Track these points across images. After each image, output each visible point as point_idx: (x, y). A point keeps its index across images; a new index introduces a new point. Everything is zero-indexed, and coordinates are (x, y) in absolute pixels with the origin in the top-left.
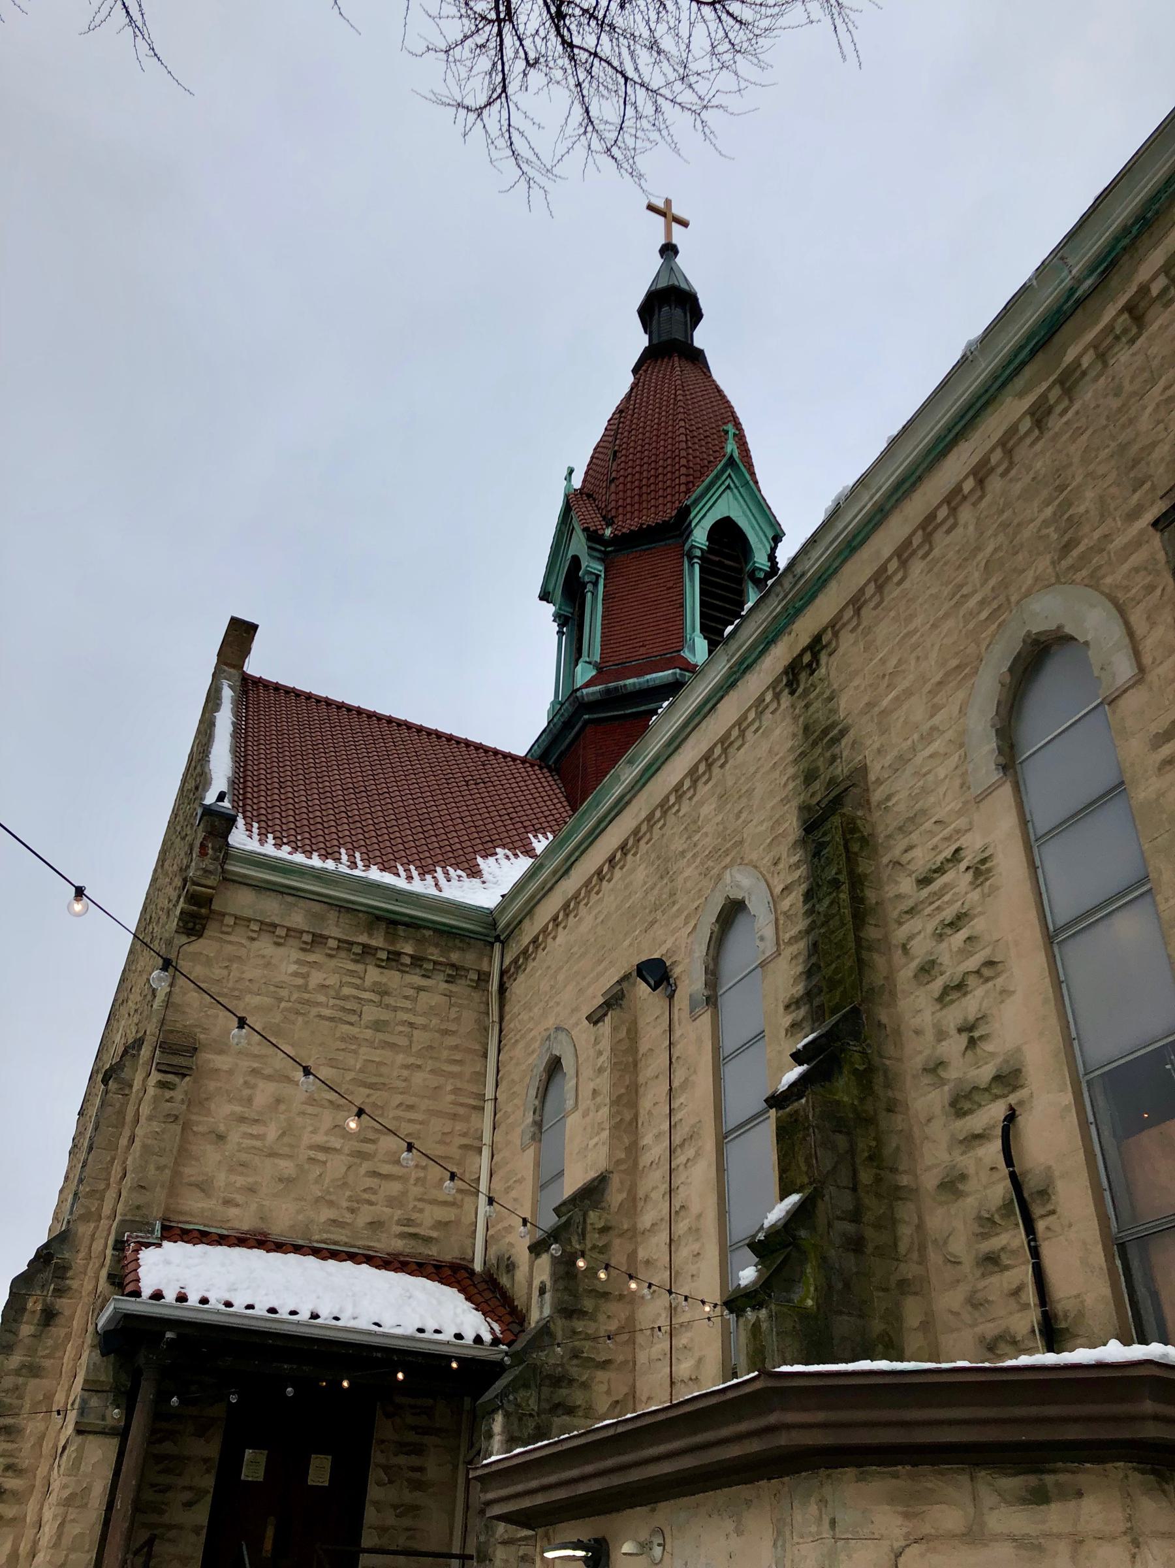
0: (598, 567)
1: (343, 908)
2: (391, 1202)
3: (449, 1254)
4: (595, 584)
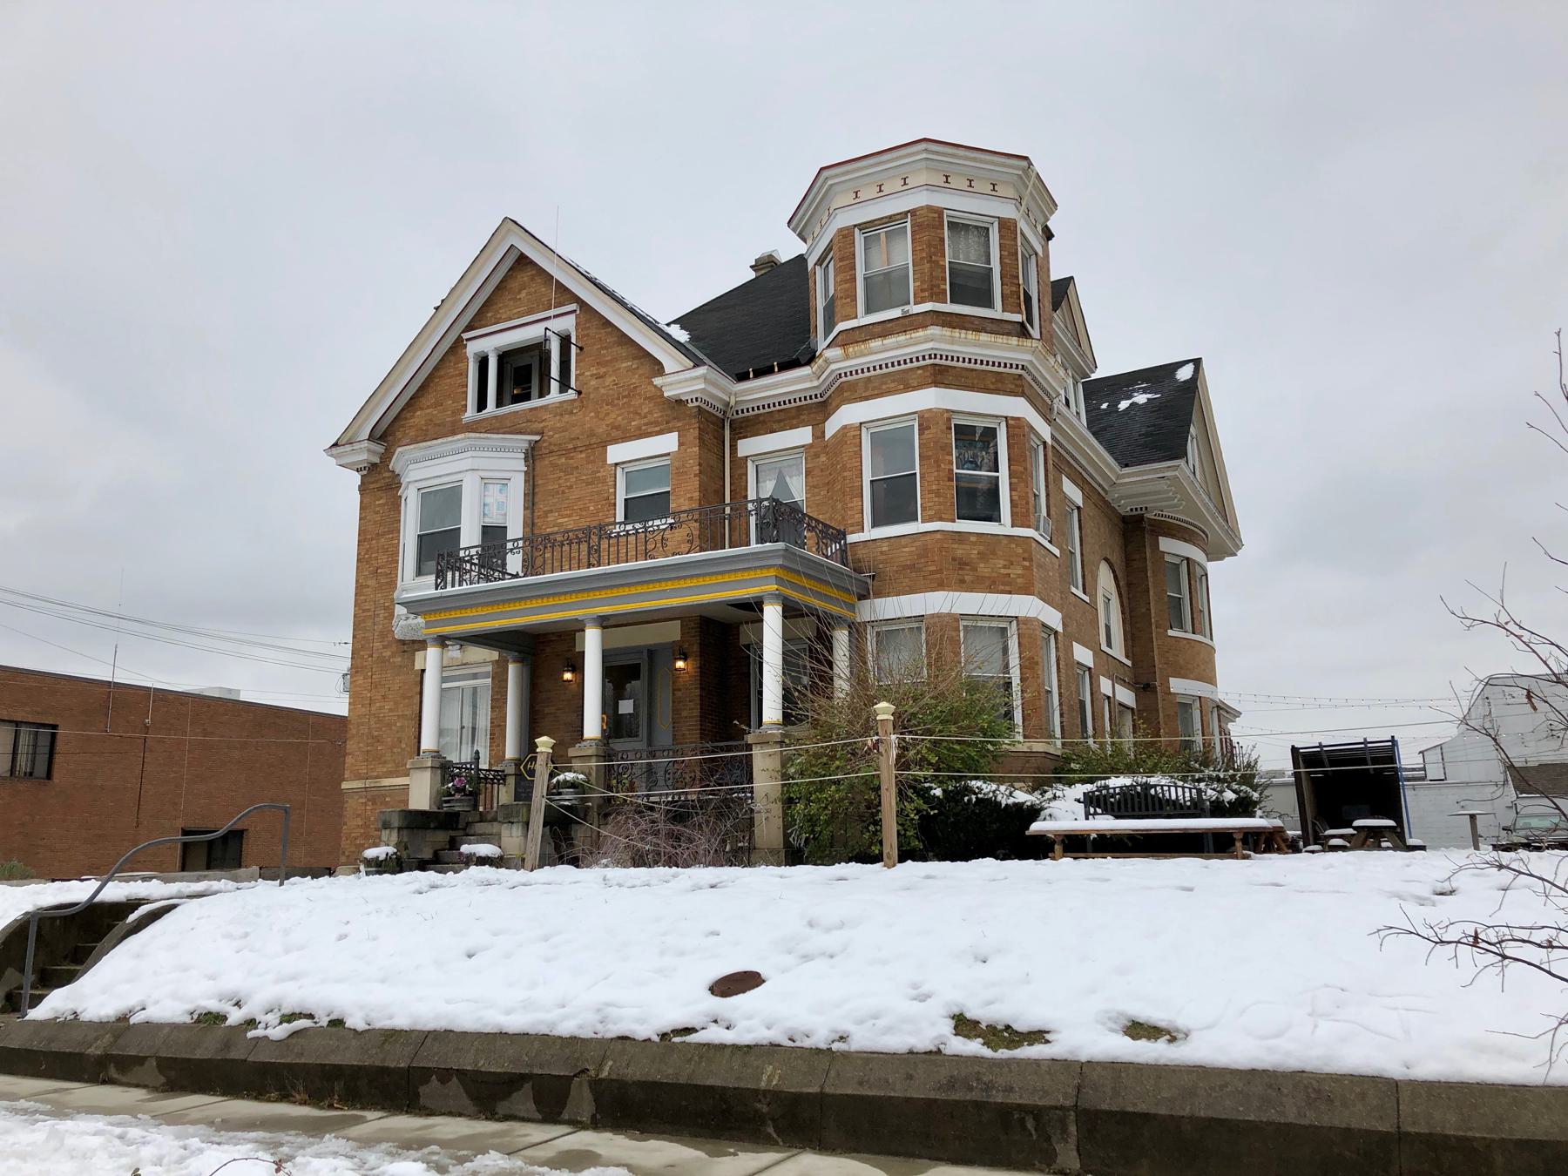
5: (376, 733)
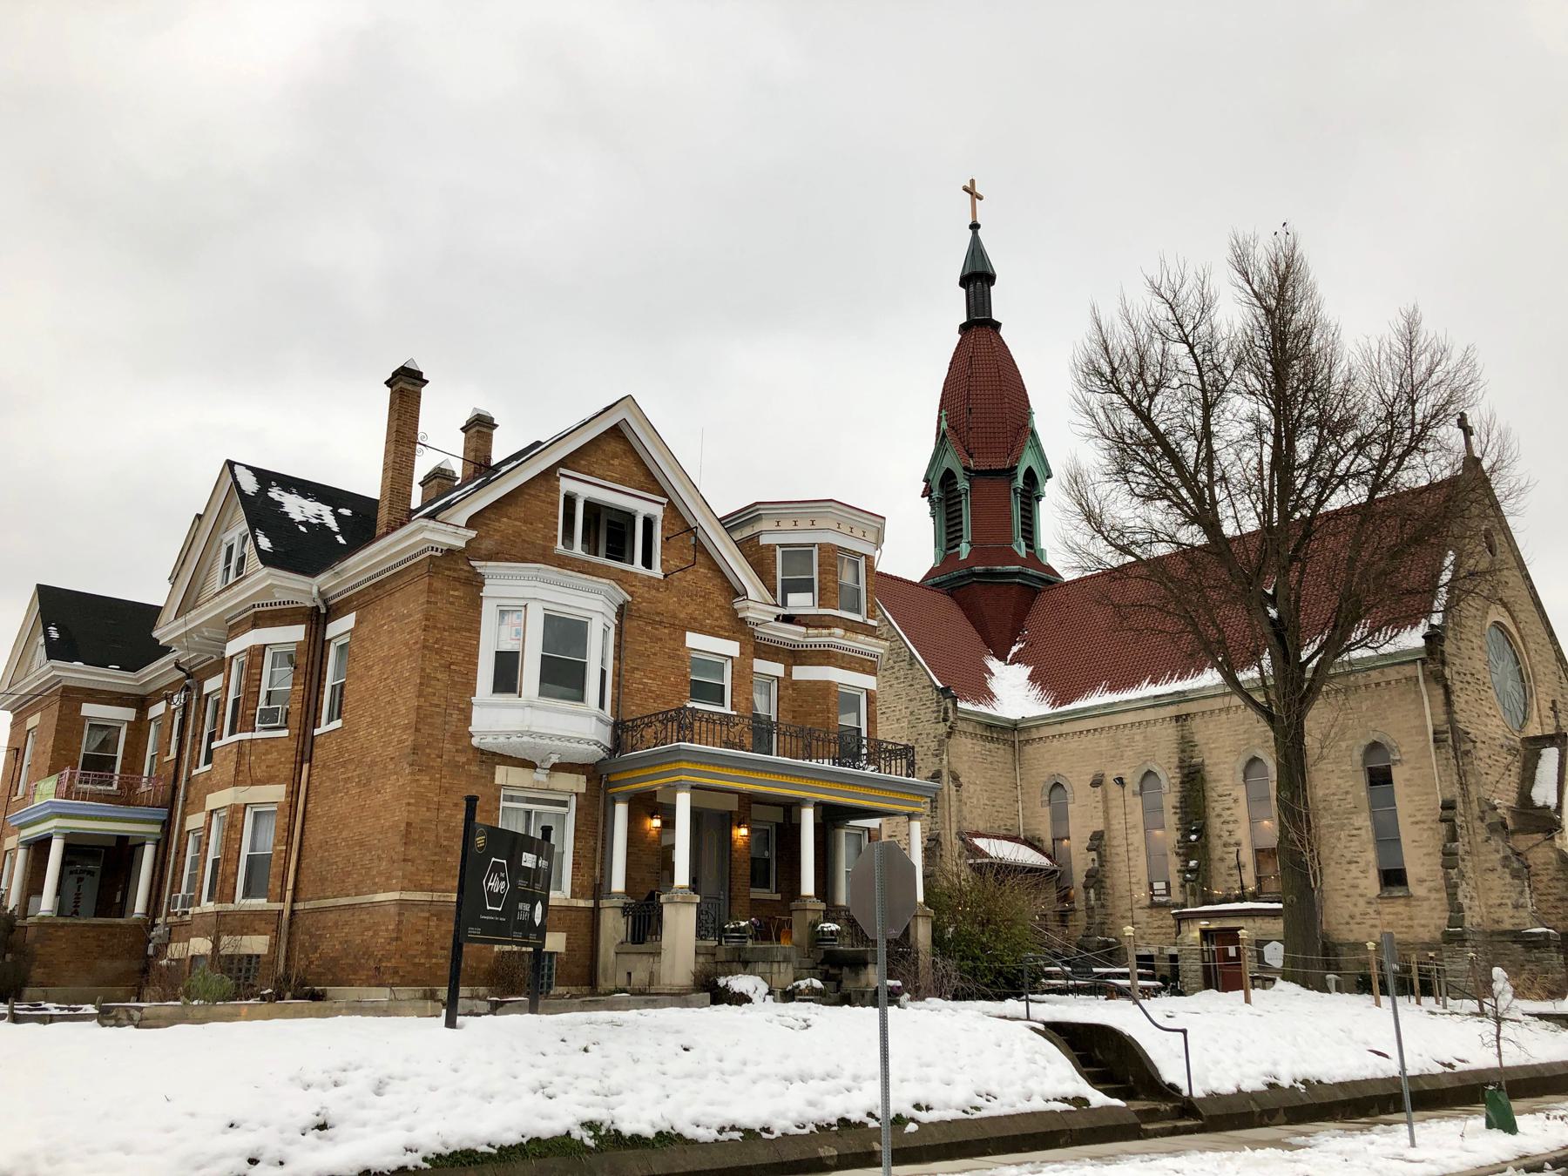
0: (967, 485)
1: (979, 723)
2: (1002, 819)
3: (1014, 834)
4: (966, 494)
5: (445, 843)
